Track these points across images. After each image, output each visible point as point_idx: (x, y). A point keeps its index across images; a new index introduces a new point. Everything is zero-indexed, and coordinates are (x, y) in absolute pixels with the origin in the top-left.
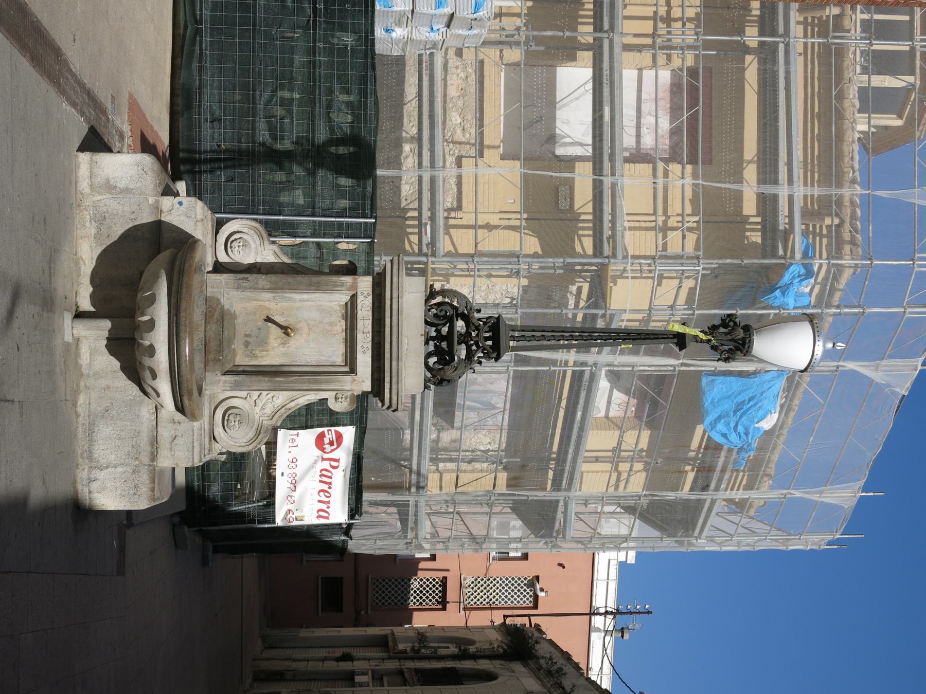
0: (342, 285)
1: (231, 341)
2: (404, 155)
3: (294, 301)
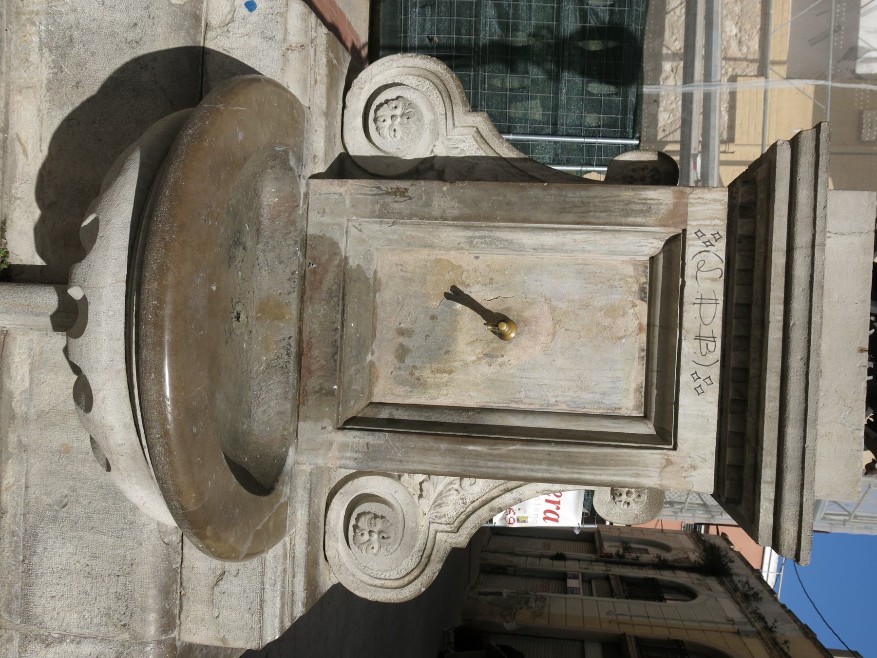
0: (647, 211)
1: (363, 345)
2: (663, 75)
3: (520, 249)
